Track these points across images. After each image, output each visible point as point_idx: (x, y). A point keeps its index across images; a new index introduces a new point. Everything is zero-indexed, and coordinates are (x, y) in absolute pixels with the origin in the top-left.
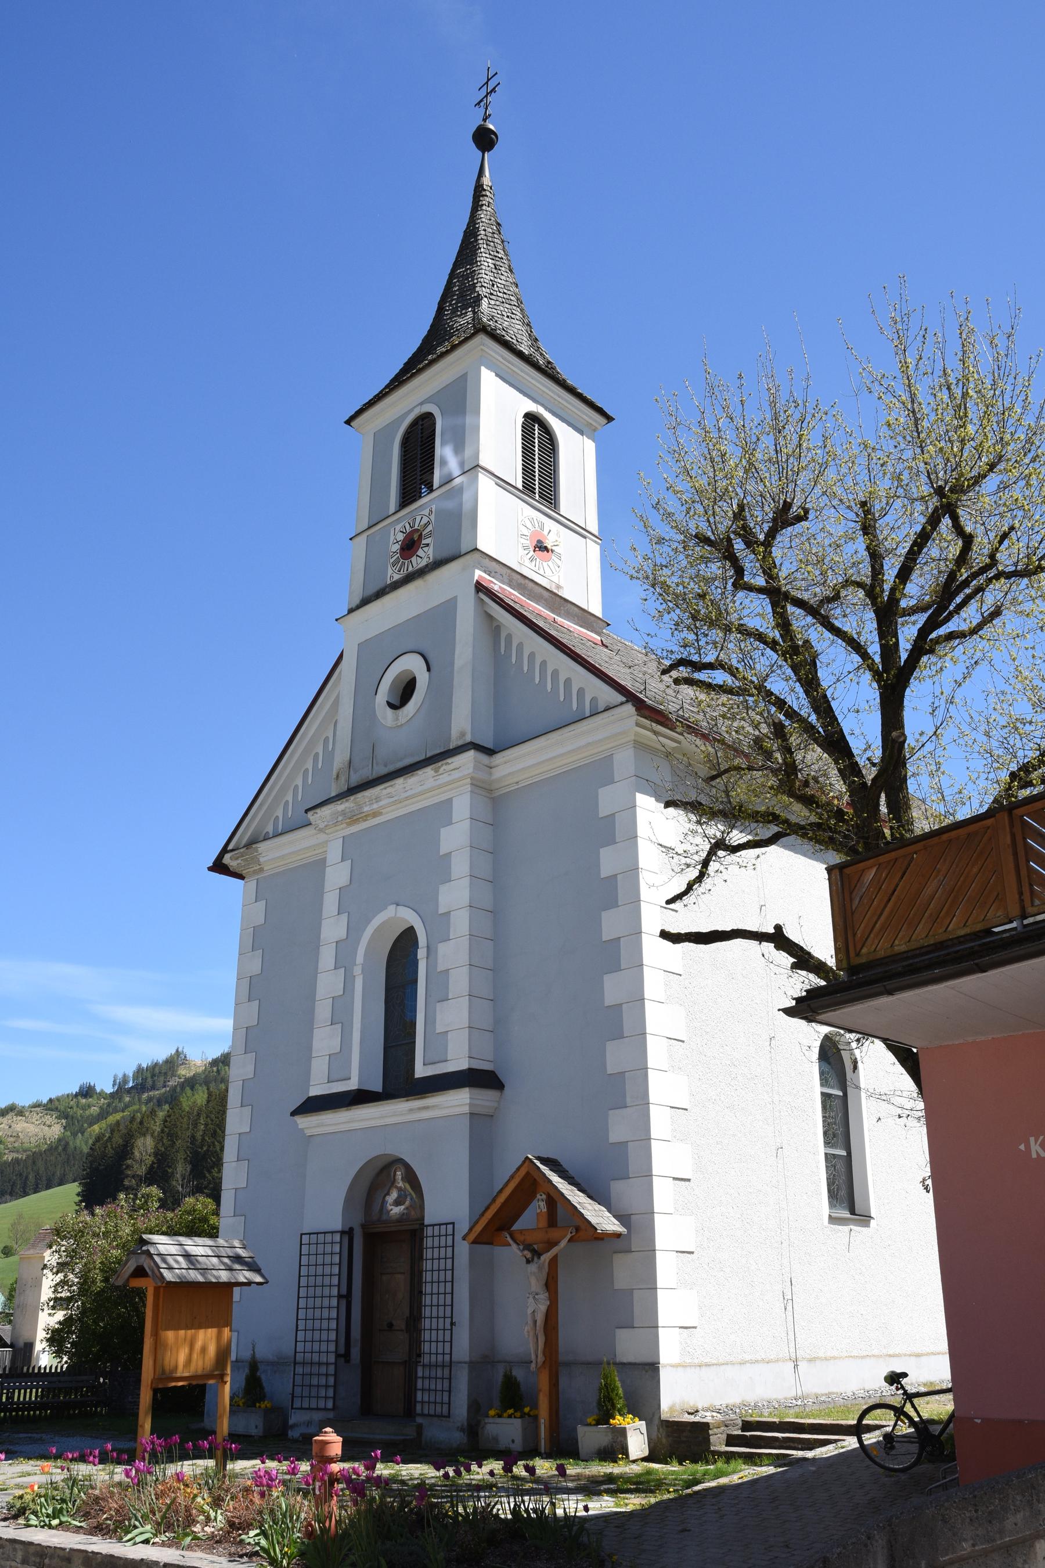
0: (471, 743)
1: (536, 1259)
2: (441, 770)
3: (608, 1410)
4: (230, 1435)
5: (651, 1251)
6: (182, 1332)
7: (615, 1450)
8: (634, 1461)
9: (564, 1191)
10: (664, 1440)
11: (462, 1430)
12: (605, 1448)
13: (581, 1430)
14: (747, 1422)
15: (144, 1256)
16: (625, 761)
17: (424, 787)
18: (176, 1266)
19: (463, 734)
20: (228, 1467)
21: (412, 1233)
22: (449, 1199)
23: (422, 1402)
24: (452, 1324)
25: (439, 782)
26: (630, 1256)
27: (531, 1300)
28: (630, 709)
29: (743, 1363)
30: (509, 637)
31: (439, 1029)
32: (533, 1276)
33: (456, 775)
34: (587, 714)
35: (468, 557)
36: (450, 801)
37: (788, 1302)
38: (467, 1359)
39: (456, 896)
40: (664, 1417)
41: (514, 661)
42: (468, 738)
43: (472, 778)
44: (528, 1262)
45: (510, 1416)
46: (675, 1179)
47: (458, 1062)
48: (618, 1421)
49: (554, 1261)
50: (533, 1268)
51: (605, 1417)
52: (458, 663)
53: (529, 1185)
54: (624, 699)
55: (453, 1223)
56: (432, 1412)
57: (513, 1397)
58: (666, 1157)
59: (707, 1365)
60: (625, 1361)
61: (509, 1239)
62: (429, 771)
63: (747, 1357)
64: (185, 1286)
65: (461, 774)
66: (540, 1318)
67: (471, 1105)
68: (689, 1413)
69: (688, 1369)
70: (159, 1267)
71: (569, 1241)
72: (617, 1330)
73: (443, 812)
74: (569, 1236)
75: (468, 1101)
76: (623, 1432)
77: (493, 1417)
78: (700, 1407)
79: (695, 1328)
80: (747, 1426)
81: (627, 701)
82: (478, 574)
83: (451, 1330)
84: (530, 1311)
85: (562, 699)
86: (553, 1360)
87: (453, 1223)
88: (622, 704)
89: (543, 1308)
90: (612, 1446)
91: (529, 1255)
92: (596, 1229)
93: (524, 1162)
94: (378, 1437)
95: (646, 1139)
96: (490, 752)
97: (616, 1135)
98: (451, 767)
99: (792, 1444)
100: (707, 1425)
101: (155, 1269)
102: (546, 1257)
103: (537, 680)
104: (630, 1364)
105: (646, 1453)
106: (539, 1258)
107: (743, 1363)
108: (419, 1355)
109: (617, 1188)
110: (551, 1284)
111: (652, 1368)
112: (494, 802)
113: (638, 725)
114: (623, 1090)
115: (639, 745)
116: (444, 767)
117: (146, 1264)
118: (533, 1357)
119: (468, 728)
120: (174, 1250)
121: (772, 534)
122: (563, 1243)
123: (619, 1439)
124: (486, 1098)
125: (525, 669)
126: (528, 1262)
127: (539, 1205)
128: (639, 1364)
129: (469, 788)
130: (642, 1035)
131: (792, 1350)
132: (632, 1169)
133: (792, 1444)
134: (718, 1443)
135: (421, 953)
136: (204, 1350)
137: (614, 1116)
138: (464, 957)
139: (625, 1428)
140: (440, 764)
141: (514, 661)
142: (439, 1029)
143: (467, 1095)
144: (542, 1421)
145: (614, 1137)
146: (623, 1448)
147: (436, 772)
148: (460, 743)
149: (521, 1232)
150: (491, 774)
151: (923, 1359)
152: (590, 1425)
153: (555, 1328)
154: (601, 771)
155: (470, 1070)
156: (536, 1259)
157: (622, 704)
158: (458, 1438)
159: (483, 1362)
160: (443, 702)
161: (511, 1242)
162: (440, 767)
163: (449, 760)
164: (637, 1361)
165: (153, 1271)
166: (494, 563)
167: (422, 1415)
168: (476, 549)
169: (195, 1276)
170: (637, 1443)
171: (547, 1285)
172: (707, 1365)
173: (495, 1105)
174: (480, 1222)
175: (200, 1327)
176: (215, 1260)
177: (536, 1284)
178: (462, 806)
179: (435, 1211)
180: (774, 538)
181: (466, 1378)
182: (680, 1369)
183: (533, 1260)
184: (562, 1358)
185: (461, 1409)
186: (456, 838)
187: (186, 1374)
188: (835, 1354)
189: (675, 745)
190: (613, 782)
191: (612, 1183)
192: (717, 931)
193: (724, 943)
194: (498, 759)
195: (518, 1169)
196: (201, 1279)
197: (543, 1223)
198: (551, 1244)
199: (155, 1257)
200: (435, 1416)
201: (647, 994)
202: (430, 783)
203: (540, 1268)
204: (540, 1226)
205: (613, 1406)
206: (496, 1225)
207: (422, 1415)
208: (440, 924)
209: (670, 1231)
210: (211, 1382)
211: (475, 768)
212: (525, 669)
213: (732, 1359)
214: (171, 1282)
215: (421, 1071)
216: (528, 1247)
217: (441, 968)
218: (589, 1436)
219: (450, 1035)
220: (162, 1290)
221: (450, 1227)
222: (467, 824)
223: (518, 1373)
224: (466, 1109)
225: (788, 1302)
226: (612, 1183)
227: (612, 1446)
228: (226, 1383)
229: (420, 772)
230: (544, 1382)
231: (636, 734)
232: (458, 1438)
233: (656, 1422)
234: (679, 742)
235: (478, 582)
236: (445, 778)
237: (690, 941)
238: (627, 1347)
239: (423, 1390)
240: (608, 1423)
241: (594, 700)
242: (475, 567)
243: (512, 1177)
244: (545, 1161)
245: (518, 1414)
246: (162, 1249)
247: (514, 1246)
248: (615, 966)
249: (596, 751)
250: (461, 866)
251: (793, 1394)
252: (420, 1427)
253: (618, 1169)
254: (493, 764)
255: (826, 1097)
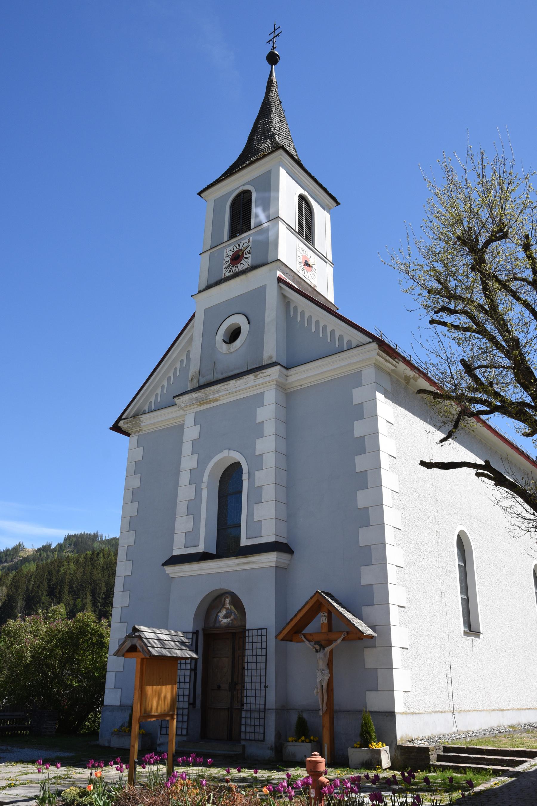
0: (275, 362)
1: (322, 650)
2: (259, 376)
3: (367, 739)
4: (176, 752)
5: (389, 647)
6: (155, 687)
7: (374, 762)
8: (385, 769)
9: (342, 611)
10: (399, 757)
11: (271, 749)
12: (366, 762)
13: (350, 751)
14: (446, 747)
15: (136, 639)
16: (369, 374)
17: (248, 385)
18: (155, 646)
19: (271, 358)
20: (175, 771)
21: (237, 635)
22: (262, 614)
23: (245, 732)
24: (266, 687)
25: (256, 383)
26: (375, 649)
27: (319, 674)
28: (374, 345)
29: (431, 713)
30: (296, 308)
31: (256, 518)
32: (321, 659)
33: (267, 379)
34: (345, 349)
35: (274, 264)
36: (262, 394)
37: (449, 678)
38: (274, 707)
39: (267, 445)
40: (399, 743)
41: (299, 320)
42: (274, 360)
43: (277, 381)
44: (317, 651)
45: (303, 741)
46: (399, 606)
47: (268, 537)
48: (374, 745)
49: (331, 652)
50: (320, 655)
51: (365, 743)
52: (267, 320)
53: (318, 605)
54: (371, 340)
55: (266, 629)
56: (252, 738)
57: (303, 730)
58: (396, 594)
59: (416, 714)
60: (372, 710)
61: (303, 638)
62: (251, 377)
63: (433, 710)
64: (162, 658)
65: (271, 379)
66: (325, 684)
67: (277, 562)
68: (410, 742)
69: (408, 715)
70: (147, 646)
71: (342, 640)
72: (367, 693)
73: (258, 399)
74: (342, 637)
75: (275, 559)
76: (378, 752)
77: (292, 741)
78: (414, 739)
79: (409, 692)
80: (446, 749)
81: (373, 341)
82: (279, 273)
83: (265, 690)
84: (318, 680)
85: (329, 340)
86: (332, 711)
87: (266, 629)
88: (369, 343)
89: (327, 678)
90: (371, 760)
91: (318, 647)
92: (363, 633)
93: (315, 594)
94: (219, 752)
95: (386, 583)
96: (287, 368)
97: (366, 580)
98: (265, 374)
99: (480, 761)
100: (428, 748)
101: (145, 648)
102: (328, 649)
103: (313, 331)
104: (376, 712)
105: (390, 765)
106: (324, 649)
107: (431, 713)
108: (243, 705)
109: (366, 610)
110: (330, 665)
111: (391, 715)
112: (288, 396)
113: (378, 354)
114: (372, 555)
115: (378, 367)
116: (261, 375)
117: (138, 643)
118: (321, 707)
119: (274, 354)
120: (152, 636)
121: (487, 244)
122: (339, 641)
123: (376, 756)
124: (285, 557)
125: (306, 324)
126: (317, 651)
127: (322, 619)
128: (382, 712)
129: (275, 386)
130: (382, 524)
131: (452, 706)
132: (376, 600)
133: (480, 761)
134: (433, 761)
135: (245, 477)
136: (165, 697)
137: (364, 570)
138: (272, 479)
139: (380, 750)
140: (258, 373)
141: (299, 320)
142: (256, 518)
143: (276, 556)
144: (326, 745)
145: (364, 582)
146: (378, 762)
147: (255, 377)
148: (269, 362)
149: (311, 634)
150: (286, 380)
151: (505, 712)
152: (356, 747)
153: (332, 690)
154: (355, 379)
155: (275, 541)
156: (322, 650)
157: (369, 343)
158: (269, 754)
159: (283, 710)
160: (257, 340)
161: (304, 640)
162: (258, 375)
163: (264, 371)
164: (380, 711)
165: (143, 648)
166: (287, 269)
167: (245, 740)
168: (279, 260)
169: (165, 652)
170: (386, 760)
171: (328, 665)
172: (416, 714)
173: (288, 562)
174: (286, 629)
175: (163, 684)
176: (172, 643)
177: (322, 664)
178: (271, 396)
179: (252, 622)
180: (486, 248)
181: (274, 719)
182: (404, 715)
183: (320, 651)
184: (336, 708)
185: (271, 737)
186: (267, 413)
187: (156, 714)
188: (469, 708)
189: (393, 368)
190: (361, 385)
191: (363, 607)
192: (453, 462)
193: (456, 469)
194: (292, 371)
195: (312, 598)
196: (169, 654)
197: (325, 629)
198: (330, 642)
199: (144, 639)
200: (254, 740)
201: (384, 502)
202: (252, 383)
203: (325, 655)
204: (324, 631)
205: (371, 737)
206: (293, 631)
207: (245, 740)
208: (257, 462)
209: (398, 637)
210: (168, 718)
211: (280, 375)
212: (306, 324)
213: (426, 710)
214: (154, 656)
215: (244, 542)
216: (317, 643)
217: (257, 484)
218: (356, 754)
219: (263, 522)
220: (145, 660)
221: (264, 631)
222: (273, 407)
223: (305, 716)
224: (274, 564)
225: (449, 678)
226: (363, 607)
227: (371, 760)
228: (174, 719)
229: (245, 377)
230: (326, 721)
231: (376, 360)
232: (269, 754)
233: (394, 746)
234: (396, 367)
235: (278, 277)
236: (260, 381)
237: (438, 467)
238: (374, 702)
239: (246, 725)
240: (367, 746)
241: (349, 342)
242: (277, 269)
243: (307, 603)
244: (327, 594)
245: (307, 740)
246: (148, 635)
247: (307, 643)
248: (364, 486)
249: (351, 368)
250: (270, 429)
251: (453, 731)
252: (244, 746)
253: (371, 598)
254: (288, 374)
255: (459, 565)
